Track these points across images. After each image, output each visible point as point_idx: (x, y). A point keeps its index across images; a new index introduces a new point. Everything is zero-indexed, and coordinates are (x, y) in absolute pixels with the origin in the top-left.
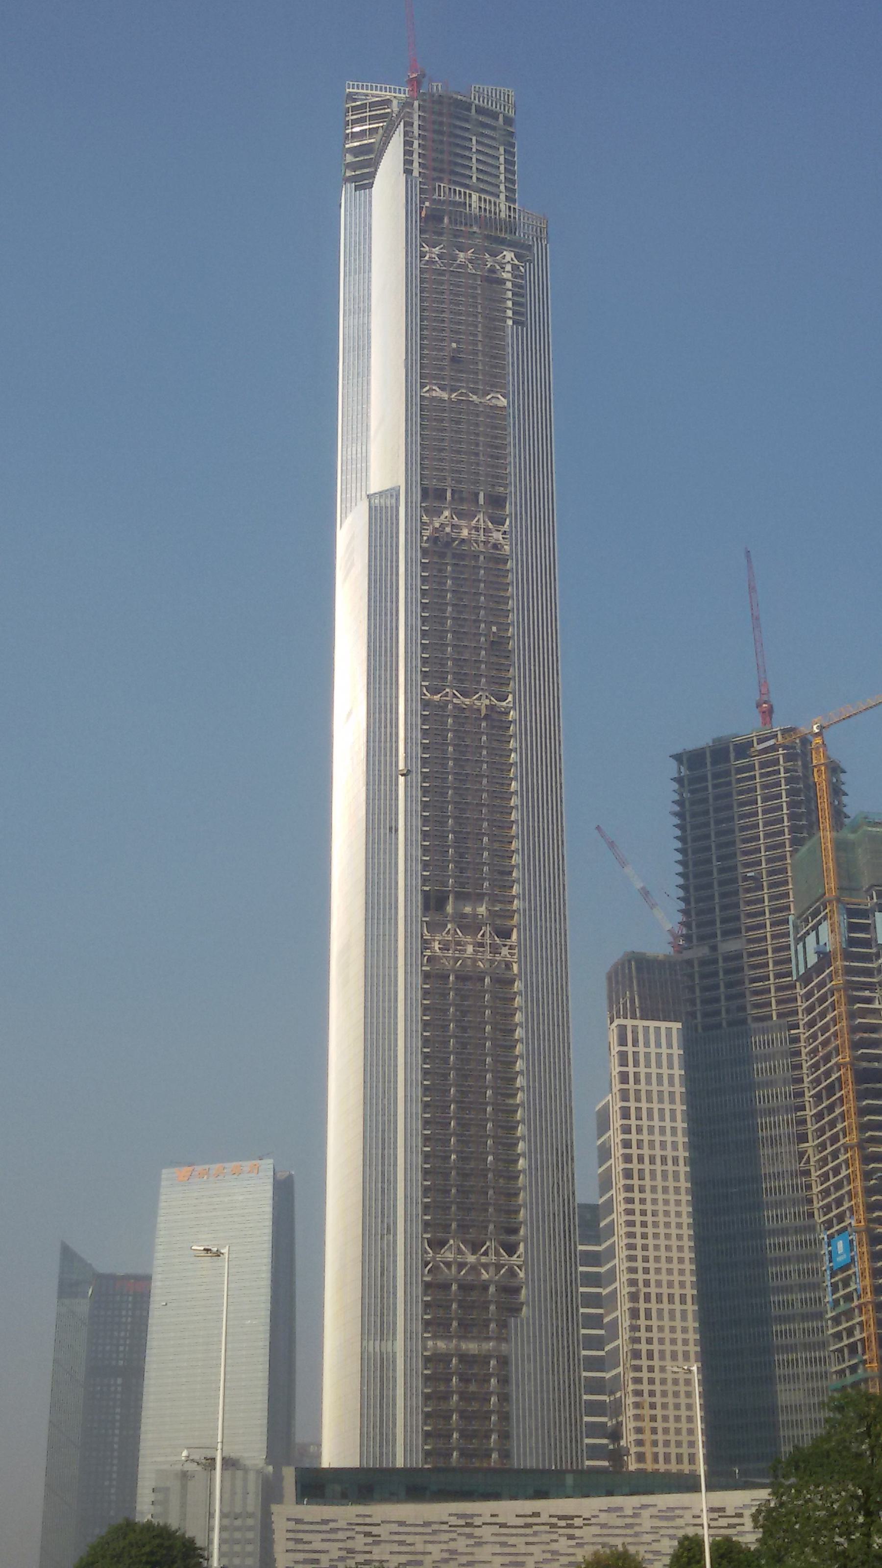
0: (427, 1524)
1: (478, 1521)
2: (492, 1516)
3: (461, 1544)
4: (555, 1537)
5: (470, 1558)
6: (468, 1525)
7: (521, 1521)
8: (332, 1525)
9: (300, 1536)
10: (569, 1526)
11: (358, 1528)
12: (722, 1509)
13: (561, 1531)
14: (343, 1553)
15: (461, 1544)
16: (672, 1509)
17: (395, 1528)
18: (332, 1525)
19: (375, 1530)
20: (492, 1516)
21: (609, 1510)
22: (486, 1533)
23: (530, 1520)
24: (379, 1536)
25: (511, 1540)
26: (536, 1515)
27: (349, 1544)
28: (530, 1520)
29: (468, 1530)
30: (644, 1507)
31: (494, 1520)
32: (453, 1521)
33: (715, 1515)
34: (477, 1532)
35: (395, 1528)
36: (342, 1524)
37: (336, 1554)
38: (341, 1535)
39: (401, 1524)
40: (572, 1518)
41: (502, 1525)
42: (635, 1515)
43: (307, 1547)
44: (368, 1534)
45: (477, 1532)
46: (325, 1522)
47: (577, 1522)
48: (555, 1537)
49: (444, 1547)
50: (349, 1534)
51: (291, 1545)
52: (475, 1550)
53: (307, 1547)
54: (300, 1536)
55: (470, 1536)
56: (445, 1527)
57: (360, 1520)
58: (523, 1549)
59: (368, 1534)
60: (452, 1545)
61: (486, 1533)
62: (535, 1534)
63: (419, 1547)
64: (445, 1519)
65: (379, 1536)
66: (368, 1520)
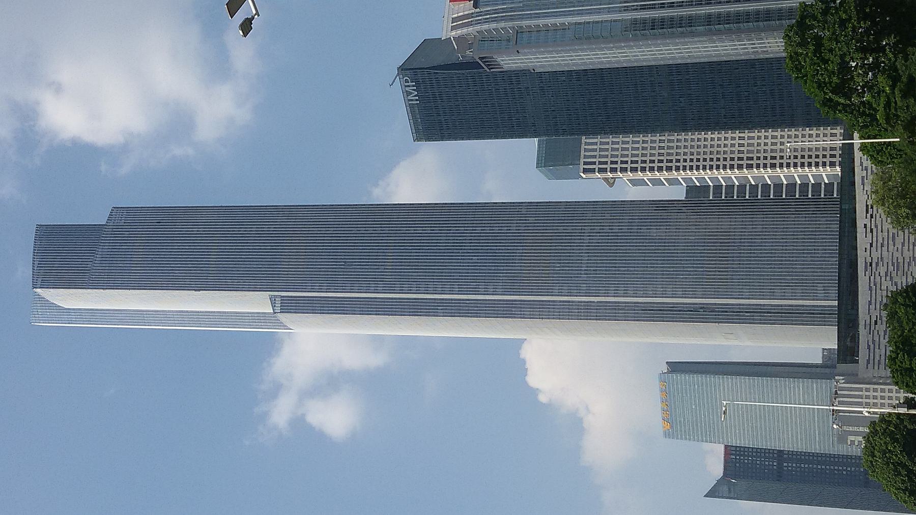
5: (890, 264)
6: (871, 265)
7: (869, 235)
8: (871, 343)
11: (873, 328)
18: (871, 343)
26: (865, 225)
28: (869, 230)
29: (874, 265)
31: (868, 251)
34: (875, 260)
35: (872, 307)
38: (876, 339)
40: (867, 206)
42: (866, 169)
45: (875, 260)
49: (883, 279)
52: (885, 261)
54: (876, 361)
55: (877, 264)
56: (872, 278)
57: (868, 328)
60: (883, 274)
61: (876, 255)
62: (876, 226)
66: (868, 322)
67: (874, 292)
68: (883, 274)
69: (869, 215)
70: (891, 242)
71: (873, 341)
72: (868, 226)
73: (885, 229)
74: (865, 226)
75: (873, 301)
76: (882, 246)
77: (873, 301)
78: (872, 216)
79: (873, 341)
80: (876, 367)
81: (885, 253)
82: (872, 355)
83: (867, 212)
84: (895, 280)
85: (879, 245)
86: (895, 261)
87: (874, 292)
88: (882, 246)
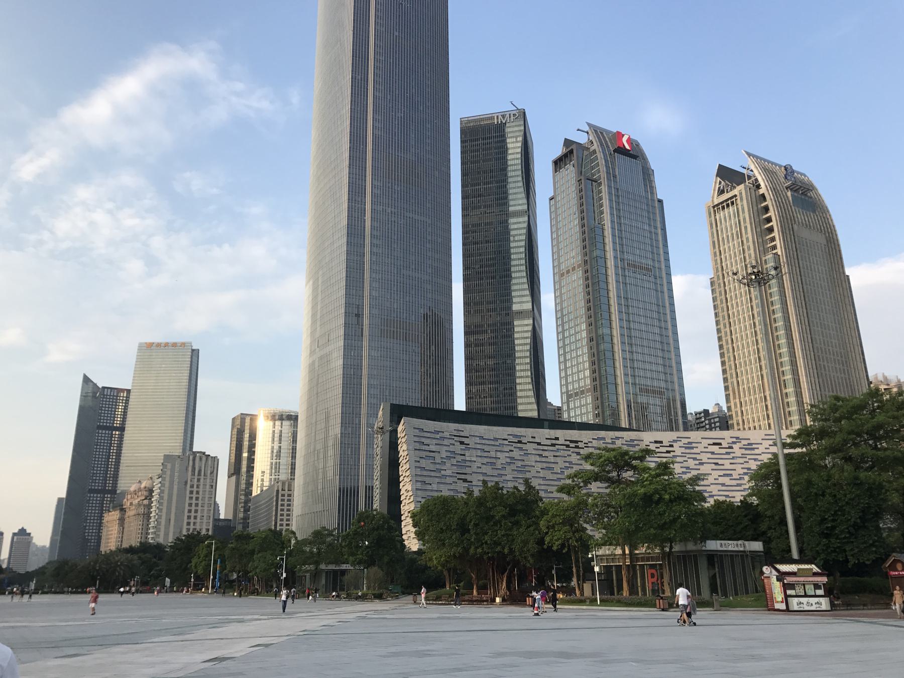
0: (496, 439)
3: (516, 454)
4: (570, 453)
6: (520, 442)
7: (549, 442)
9: (423, 440)
10: (577, 447)
12: (661, 442)
13: (572, 450)
14: (449, 454)
15: (516, 454)
16: (632, 440)
17: (478, 440)
18: (441, 435)
19: (466, 441)
21: (599, 439)
23: (554, 442)
25: (545, 454)
26: (557, 439)
27: (452, 448)
28: (554, 442)
29: (519, 445)
30: (618, 438)
31: (531, 440)
33: (658, 445)
36: (446, 434)
37: (444, 455)
38: (446, 442)
39: (481, 438)
40: (576, 442)
41: (539, 444)
43: (426, 448)
44: (462, 443)
46: (437, 432)
47: (580, 445)
48: (570, 453)
51: (418, 446)
53: (426, 448)
54: (423, 440)
55: (521, 449)
56: (506, 442)
58: (552, 459)
61: (530, 448)
63: (493, 454)
64: (506, 437)
66: (462, 434)
67: (493, 443)
69: (568, 443)
70: (545, 465)
71: (443, 438)
72: (557, 442)
73: (558, 460)
74: (557, 439)
75: (484, 442)
76: (540, 455)
77: (484, 442)
78: (568, 446)
79: (443, 438)
80: (417, 439)
82: (429, 435)
83: (571, 441)
84: (508, 467)
85: (541, 453)
86: (527, 469)
87: (493, 443)
88: (540, 455)
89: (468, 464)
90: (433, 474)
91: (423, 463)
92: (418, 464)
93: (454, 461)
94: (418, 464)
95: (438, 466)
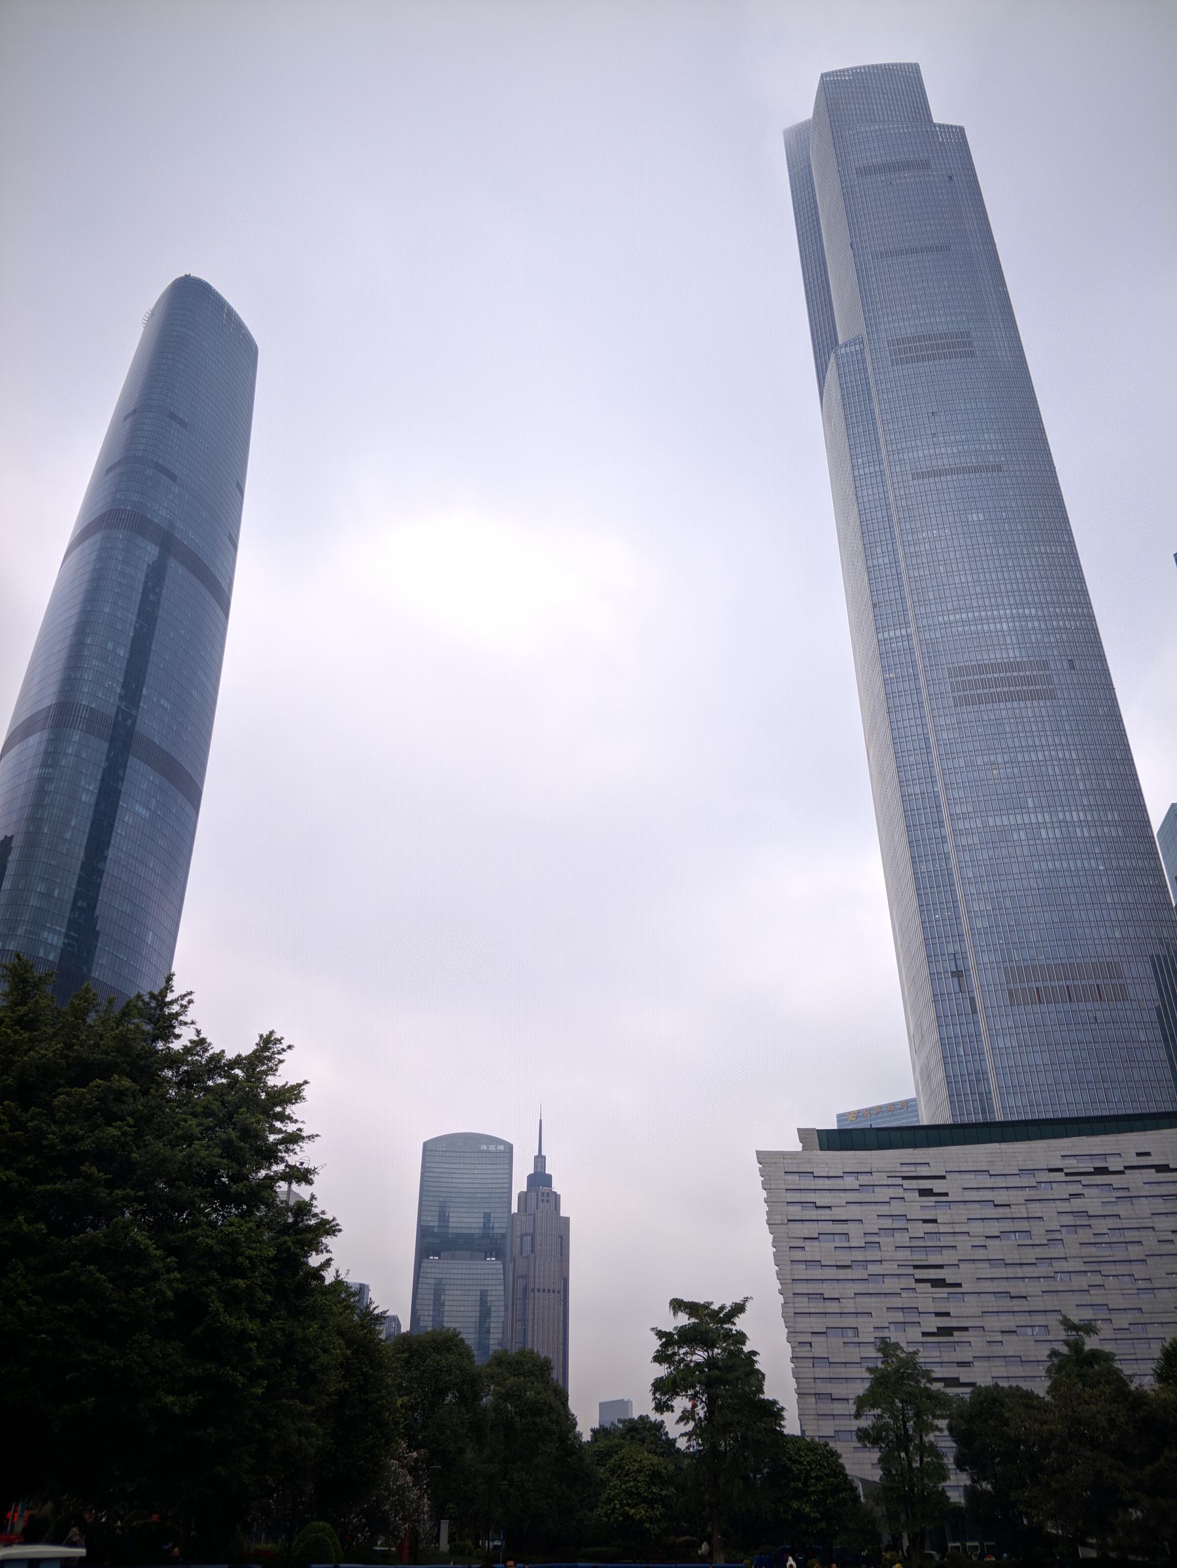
1: (1114, 1164)
2: (1138, 1154)
6: (1103, 1171)
8: (864, 1179)
11: (908, 1184)
19: (937, 1186)
20: (1138, 1154)
22: (1135, 1180)
24: (946, 1194)
27: (896, 1208)
31: (1143, 1161)
32: (1072, 1164)
37: (873, 1225)
38: (882, 1194)
43: (824, 1214)
44: (924, 1193)
49: (1064, 1207)
50: (893, 1192)
56: (1060, 1176)
59: (924, 1193)
64: (1058, 1164)
65: (946, 1194)
66: (924, 1171)
68: (1076, 1204)
81: (1145, 1207)
89: (945, 1241)
90: (842, 1274)
91: (812, 1251)
92: (799, 1255)
93: (902, 1238)
94: (799, 1255)
95: (859, 1255)
